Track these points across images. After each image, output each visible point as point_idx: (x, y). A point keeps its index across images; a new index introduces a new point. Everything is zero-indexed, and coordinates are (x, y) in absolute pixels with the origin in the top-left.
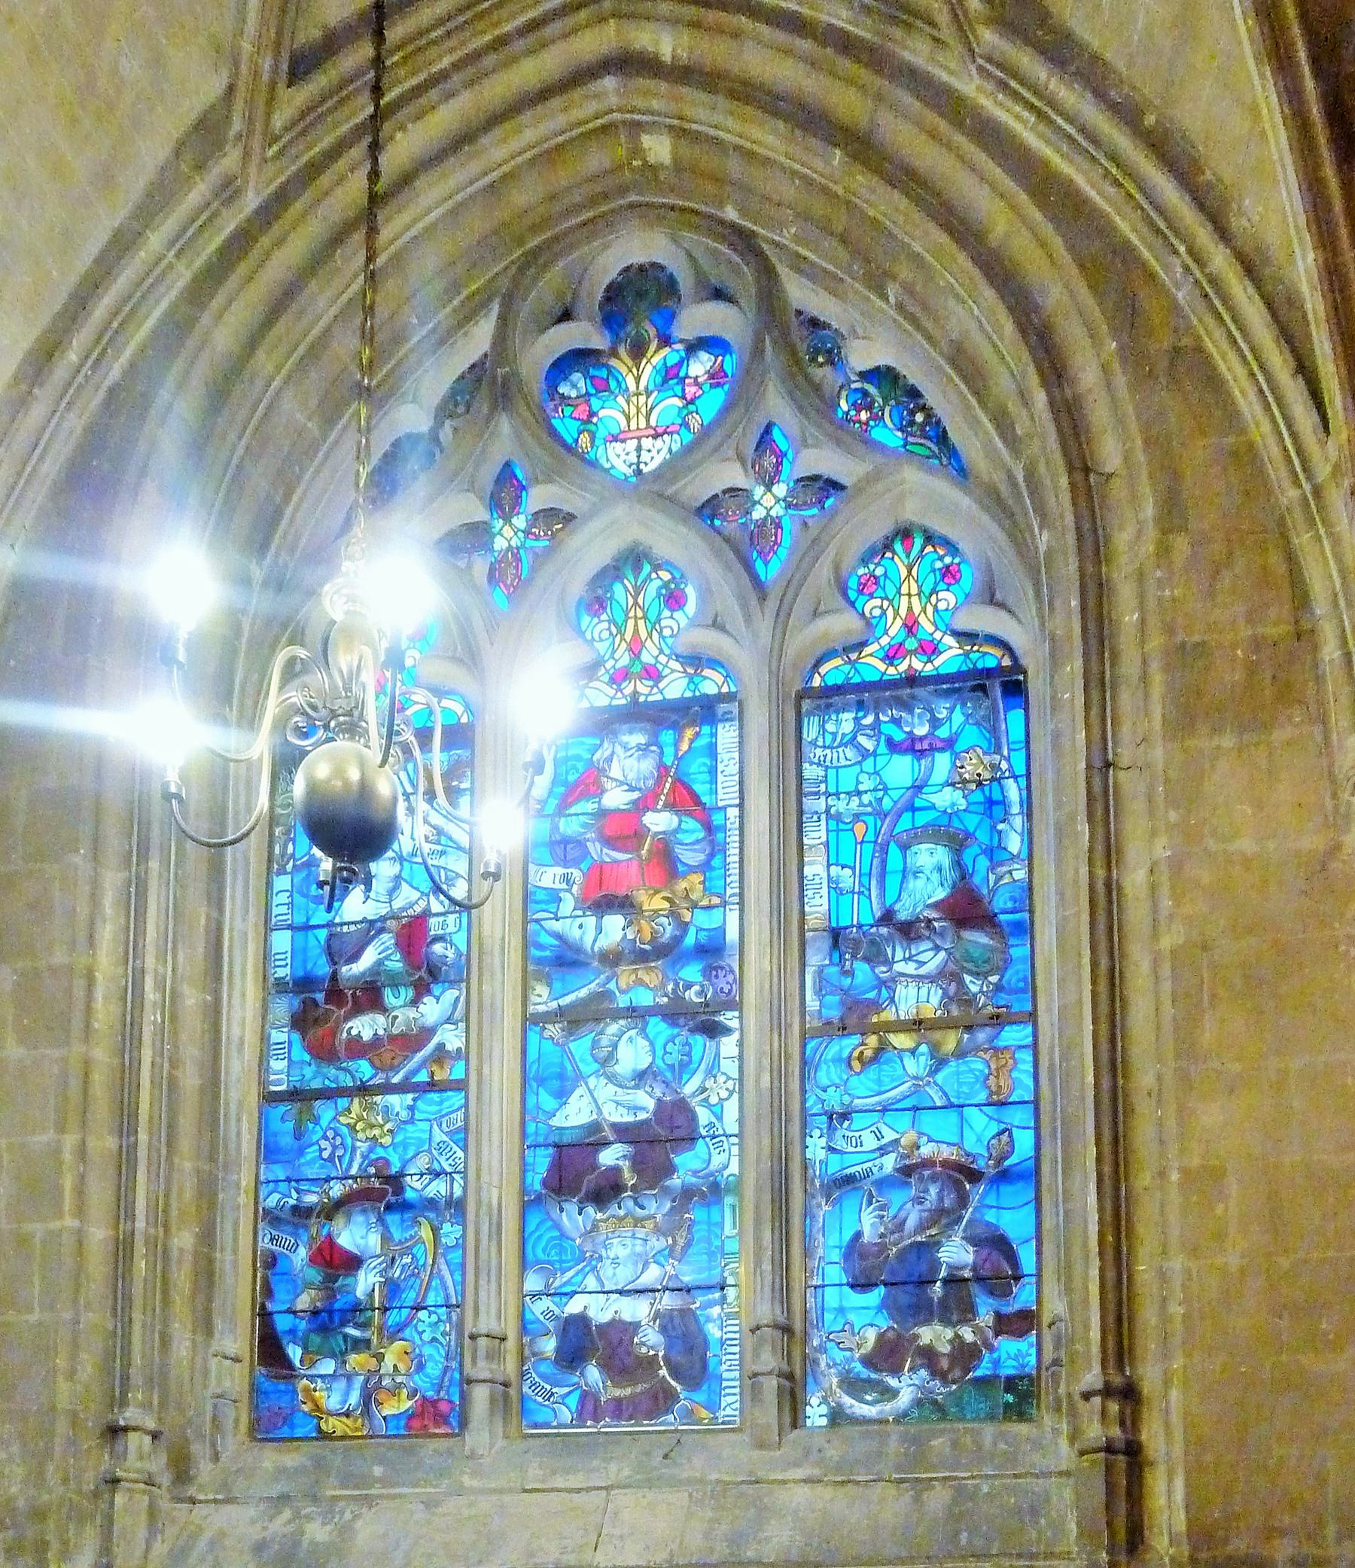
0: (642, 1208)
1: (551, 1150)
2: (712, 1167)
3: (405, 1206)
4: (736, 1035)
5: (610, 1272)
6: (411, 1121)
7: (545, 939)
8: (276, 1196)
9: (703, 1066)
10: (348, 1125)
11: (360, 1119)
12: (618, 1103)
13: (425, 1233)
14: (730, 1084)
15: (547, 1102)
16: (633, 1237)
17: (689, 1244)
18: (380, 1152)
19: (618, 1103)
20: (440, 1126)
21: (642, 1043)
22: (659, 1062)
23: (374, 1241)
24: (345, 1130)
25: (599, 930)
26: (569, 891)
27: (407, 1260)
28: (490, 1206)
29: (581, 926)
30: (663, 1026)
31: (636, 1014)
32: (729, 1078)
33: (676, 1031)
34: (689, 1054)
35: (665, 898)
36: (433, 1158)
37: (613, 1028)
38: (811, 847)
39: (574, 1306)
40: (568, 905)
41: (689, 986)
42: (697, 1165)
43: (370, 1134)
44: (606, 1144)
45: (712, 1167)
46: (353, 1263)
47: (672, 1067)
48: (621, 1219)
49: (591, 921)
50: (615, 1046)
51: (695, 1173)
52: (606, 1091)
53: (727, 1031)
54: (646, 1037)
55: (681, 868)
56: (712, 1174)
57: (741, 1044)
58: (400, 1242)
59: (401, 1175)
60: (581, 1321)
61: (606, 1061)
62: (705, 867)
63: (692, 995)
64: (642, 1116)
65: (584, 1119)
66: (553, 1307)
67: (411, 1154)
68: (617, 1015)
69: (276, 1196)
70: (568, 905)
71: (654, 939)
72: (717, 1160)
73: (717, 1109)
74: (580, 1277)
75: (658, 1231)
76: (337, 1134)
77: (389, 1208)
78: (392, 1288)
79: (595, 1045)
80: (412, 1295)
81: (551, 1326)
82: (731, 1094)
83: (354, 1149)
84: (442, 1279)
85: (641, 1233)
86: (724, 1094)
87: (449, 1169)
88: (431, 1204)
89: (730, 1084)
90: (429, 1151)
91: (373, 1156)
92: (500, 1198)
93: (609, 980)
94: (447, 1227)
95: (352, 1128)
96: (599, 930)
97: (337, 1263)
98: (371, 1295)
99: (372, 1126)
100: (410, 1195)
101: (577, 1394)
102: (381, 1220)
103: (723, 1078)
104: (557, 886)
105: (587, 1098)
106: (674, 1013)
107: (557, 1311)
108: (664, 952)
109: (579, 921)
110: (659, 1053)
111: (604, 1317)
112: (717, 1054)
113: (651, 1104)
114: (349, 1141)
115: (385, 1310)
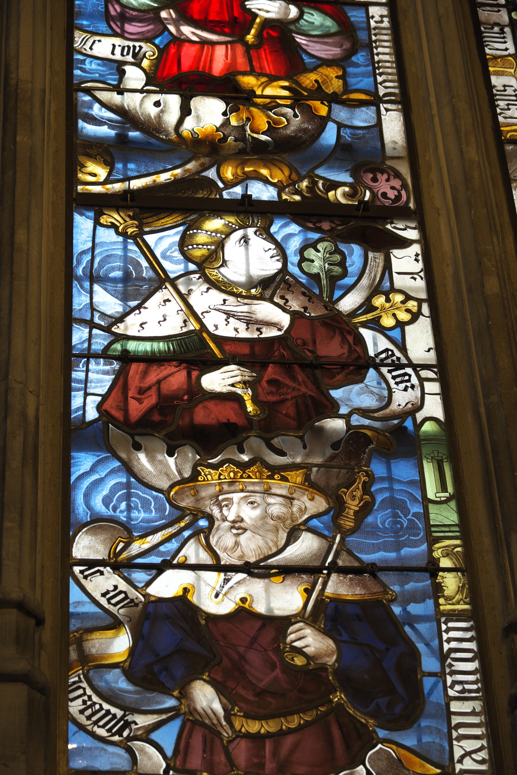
0: (282, 453)
1: (116, 365)
2: (394, 407)
4: (416, 248)
5: (229, 540)
7: (97, 110)
9: (365, 281)
12: (229, 315)
14: (412, 305)
15: (108, 302)
16: (267, 492)
17: (366, 509)
19: (229, 315)
21: (259, 244)
22: (293, 269)
25: (185, 111)
26: (138, 65)
28: (24, 414)
29: (157, 104)
30: (294, 228)
31: (250, 211)
32: (408, 298)
33: (316, 236)
34: (342, 264)
35: (284, 88)
37: (215, 224)
38: (495, 57)
39: (168, 585)
40: (135, 77)
41: (334, 185)
42: (368, 402)
44: (215, 364)
45: (394, 407)
47: (316, 277)
48: (243, 466)
49: (173, 102)
50: (221, 245)
51: (364, 412)
52: (204, 299)
53: (405, 243)
54: (271, 238)
55: (307, 60)
56: (394, 416)
57: (427, 257)
60: (182, 606)
61: (206, 265)
62: (341, 63)
63: (338, 195)
64: (270, 333)
65: (174, 326)
66: (123, 586)
68: (222, 208)
70: (135, 77)
71: (270, 131)
72: (402, 398)
73: (396, 334)
74: (173, 545)
75: (311, 485)
79: (183, 244)
81: (120, 612)
82: (415, 317)
85: (280, 488)
86: (404, 317)
89: (412, 305)
92: (37, 410)
93: (206, 168)
96: (185, 111)
101: (174, 727)
103: (398, 298)
104: (118, 56)
105: (176, 304)
106: (311, 212)
107: (133, 594)
108: (281, 149)
109: (156, 97)
110: (293, 259)
111: (224, 607)
112: (388, 266)
113: (285, 320)
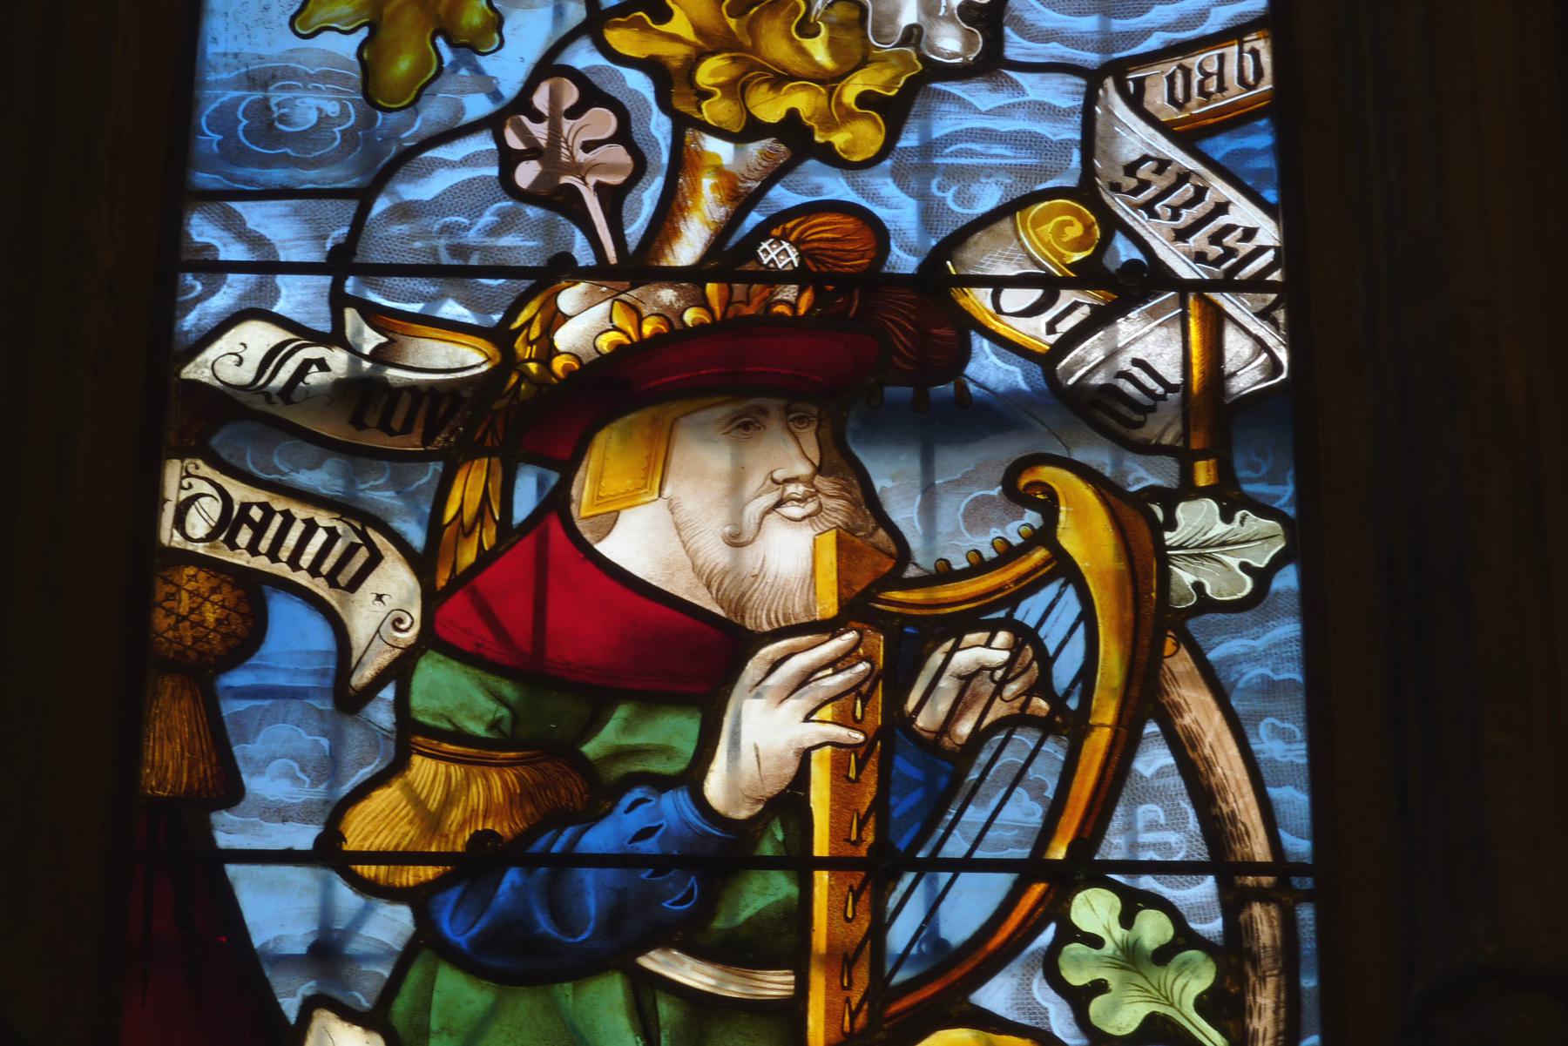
3: (985, 416)
6: (989, 64)
8: (257, 338)
10: (651, 66)
11: (710, 42)
13: (1087, 534)
18: (836, 187)
20: (1135, 102)
23: (792, 557)
24: (638, 83)
27: (982, 651)
36: (1111, 224)
43: (770, 108)
46: (699, 653)
58: (944, 574)
59: (939, 278)
67: (989, 197)
69: (257, 338)
76: (592, 95)
77: (889, 426)
78: (907, 781)
80: (1024, 812)
83: (682, 162)
84: (1183, 747)
87: (1186, 270)
88: (1108, 410)
90: (1086, 192)
91: (783, 197)
94: (1197, 519)
95: (670, 80)
97: (607, 664)
98: (789, 802)
99: (780, 79)
100: (989, 369)
102: (841, 466)
114: (659, 127)
115: (876, 869)
